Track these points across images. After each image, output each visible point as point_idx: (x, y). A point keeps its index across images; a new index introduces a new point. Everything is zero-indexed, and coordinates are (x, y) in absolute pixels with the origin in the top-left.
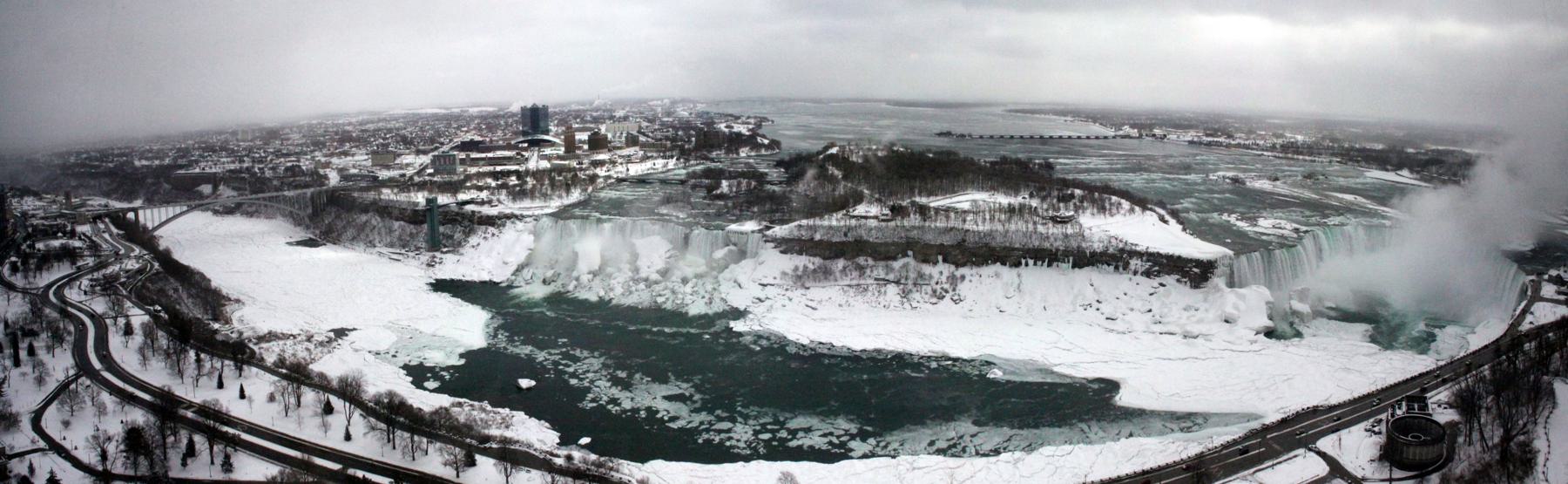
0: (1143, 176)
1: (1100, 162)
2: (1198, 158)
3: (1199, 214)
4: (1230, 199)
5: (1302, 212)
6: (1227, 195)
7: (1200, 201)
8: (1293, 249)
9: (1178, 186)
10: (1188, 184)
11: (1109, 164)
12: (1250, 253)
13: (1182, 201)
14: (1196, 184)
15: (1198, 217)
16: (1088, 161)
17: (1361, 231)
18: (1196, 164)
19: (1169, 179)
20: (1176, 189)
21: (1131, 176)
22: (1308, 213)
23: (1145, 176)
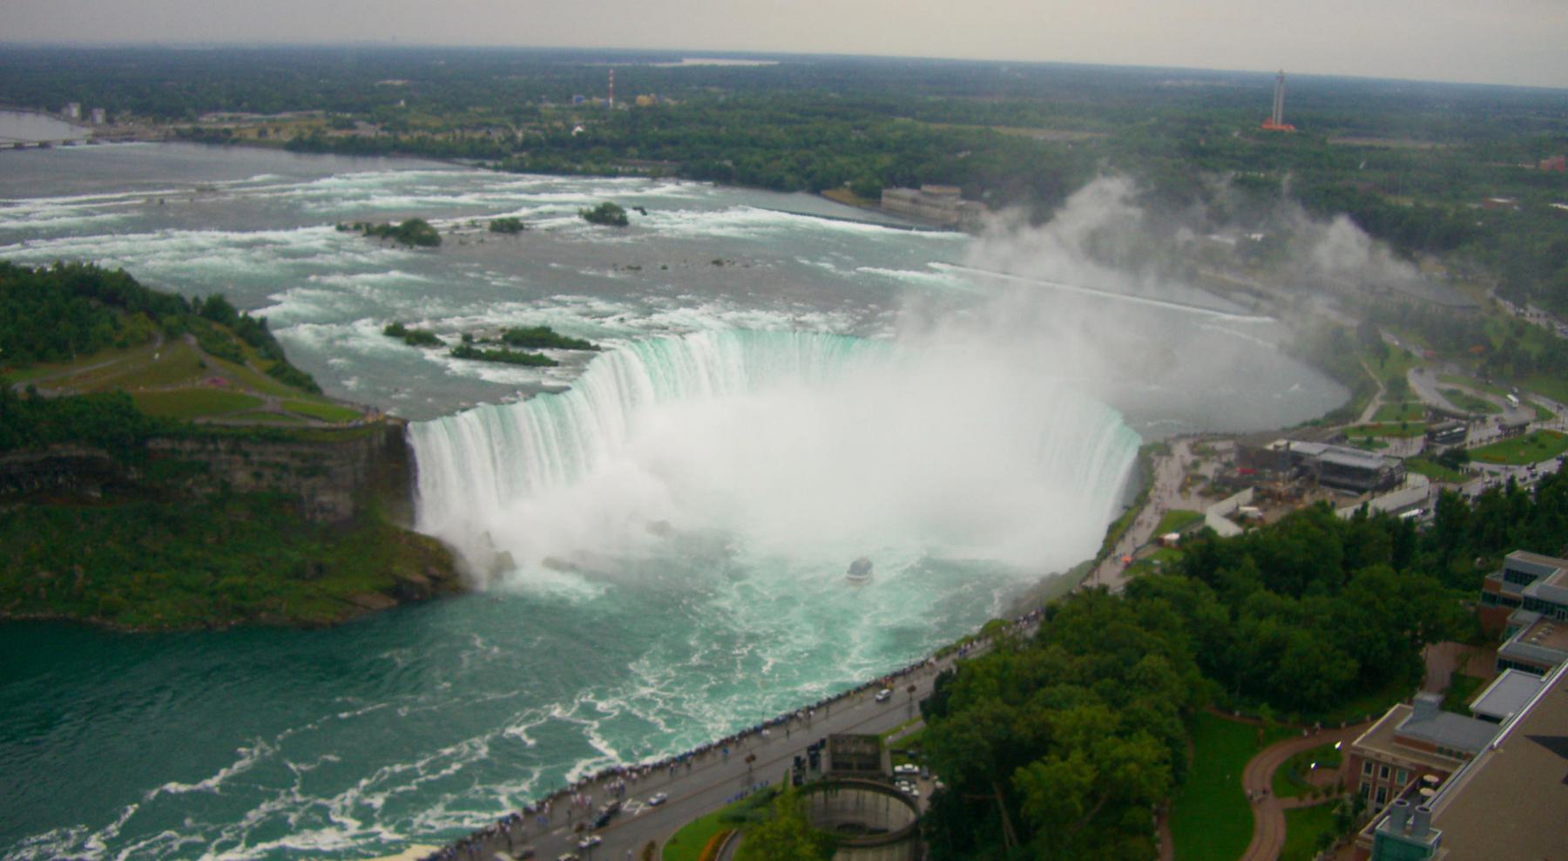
0: (173, 241)
1: (48, 210)
2: (316, 184)
3: (323, 328)
4: (398, 281)
5: (585, 304)
6: (395, 275)
7: (328, 294)
8: (561, 398)
9: (272, 267)
10: (293, 254)
11: (85, 213)
12: (451, 413)
13: (276, 297)
14: (312, 253)
15: (318, 333)
16: (24, 208)
17: (733, 345)
18: (316, 199)
19: (238, 245)
20: (259, 270)
21: (140, 242)
22: (599, 305)
23: (179, 238)
